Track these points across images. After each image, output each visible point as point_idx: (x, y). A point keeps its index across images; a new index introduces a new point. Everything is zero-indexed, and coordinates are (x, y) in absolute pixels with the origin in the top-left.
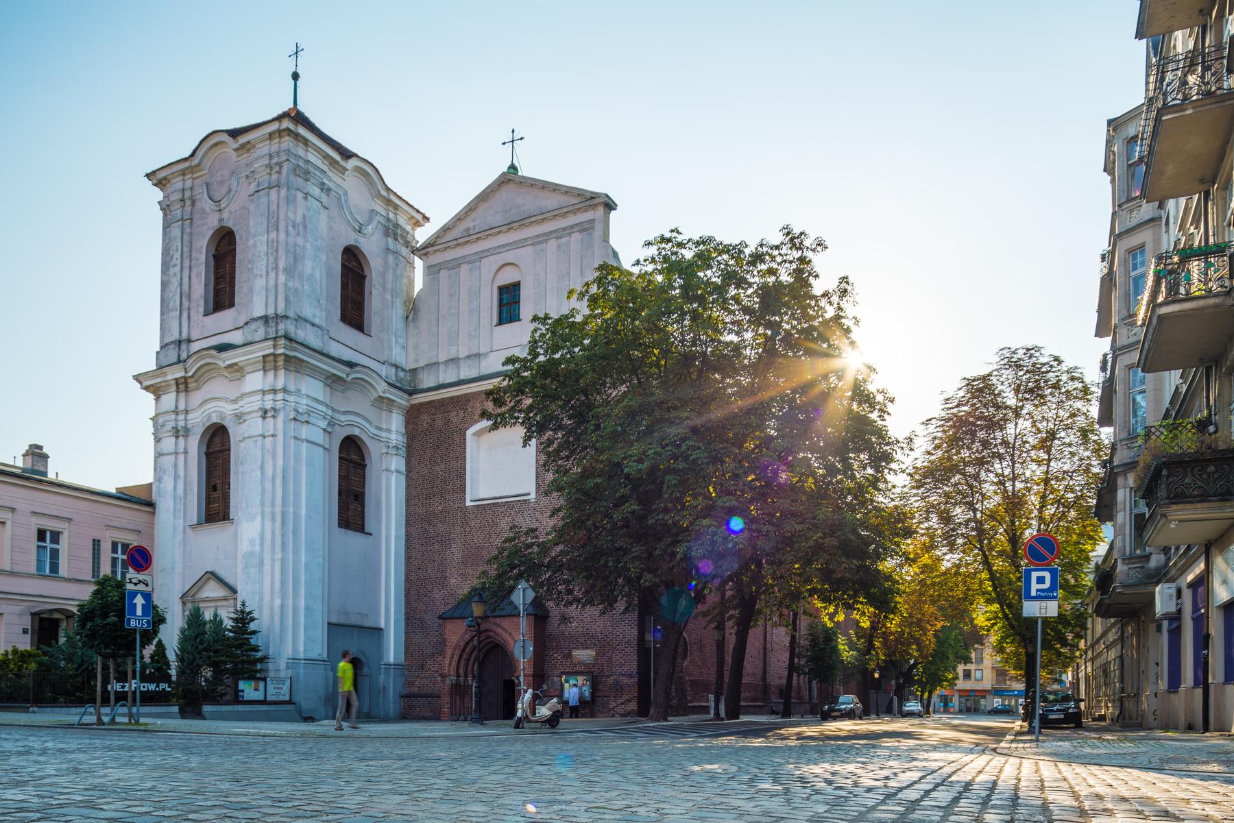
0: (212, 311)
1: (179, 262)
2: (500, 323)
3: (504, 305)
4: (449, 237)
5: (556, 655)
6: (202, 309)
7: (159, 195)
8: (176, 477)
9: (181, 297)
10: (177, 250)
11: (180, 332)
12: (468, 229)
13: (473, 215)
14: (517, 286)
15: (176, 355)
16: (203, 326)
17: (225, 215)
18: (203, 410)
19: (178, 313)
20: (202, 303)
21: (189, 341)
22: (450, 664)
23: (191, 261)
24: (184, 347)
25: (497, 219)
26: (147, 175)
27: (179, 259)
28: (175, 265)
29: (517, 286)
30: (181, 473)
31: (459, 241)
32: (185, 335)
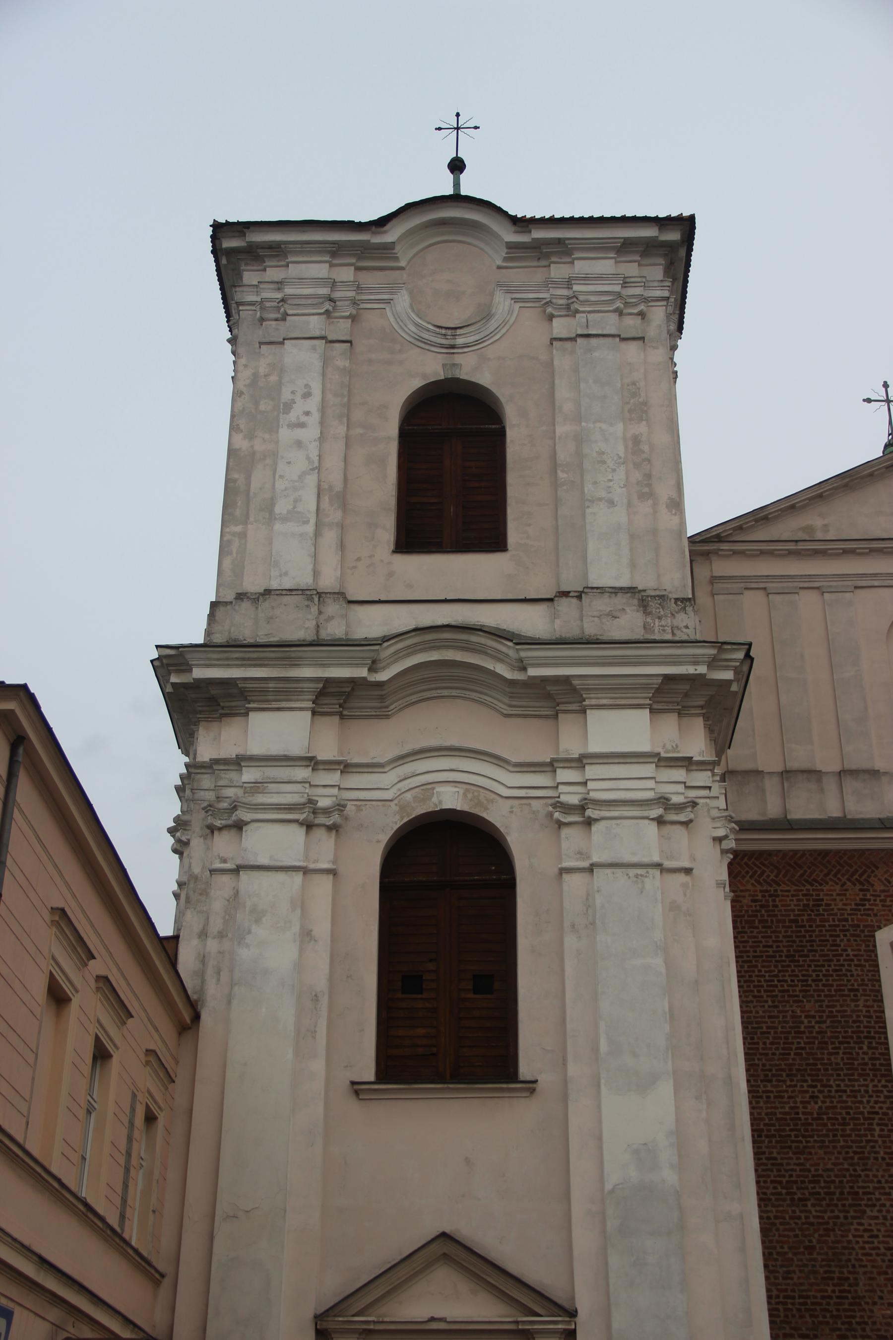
8: (307, 935)
15: (311, 624)
19: (310, 528)
30: (323, 928)
31: (801, 546)
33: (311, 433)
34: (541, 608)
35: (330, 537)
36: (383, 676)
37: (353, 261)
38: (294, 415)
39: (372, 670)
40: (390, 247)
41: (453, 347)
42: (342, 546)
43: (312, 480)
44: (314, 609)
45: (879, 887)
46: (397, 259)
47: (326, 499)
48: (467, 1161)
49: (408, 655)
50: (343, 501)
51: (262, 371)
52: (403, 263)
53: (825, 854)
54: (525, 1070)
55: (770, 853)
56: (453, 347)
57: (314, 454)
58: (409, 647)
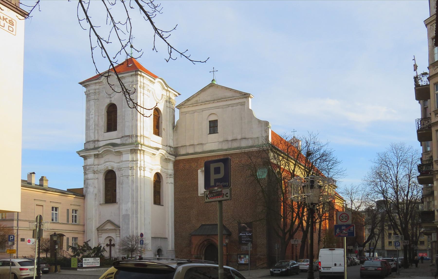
0: (106, 132)
1: (94, 114)
2: (210, 133)
3: (211, 127)
4: (189, 103)
5: (234, 248)
6: (103, 130)
7: (85, 89)
9: (95, 125)
10: (93, 109)
11: (95, 137)
12: (197, 101)
13: (198, 96)
14: (216, 121)
15: (94, 146)
16: (104, 136)
17: (113, 99)
18: (105, 164)
19: (94, 131)
20: (103, 128)
21: (98, 141)
22: (194, 251)
23: (99, 113)
24: (96, 142)
25: (209, 98)
26: (81, 83)
27: (94, 113)
28: (92, 115)
29: (216, 121)
32: (96, 139)
33: (93, 116)
34: (120, 139)
35: (96, 131)
36: (100, 153)
37: (98, 84)
38: (91, 113)
39: (99, 152)
40: (102, 82)
41: (111, 98)
42: (98, 133)
43: (94, 123)
44: (94, 143)
45: (199, 163)
46: (103, 83)
47: (96, 126)
48: (111, 212)
49: (103, 149)
50: (98, 126)
51: (88, 106)
52: (104, 84)
53: (192, 158)
54: (117, 201)
55: (185, 159)
56: (111, 98)
57: (94, 119)
58: (104, 148)
